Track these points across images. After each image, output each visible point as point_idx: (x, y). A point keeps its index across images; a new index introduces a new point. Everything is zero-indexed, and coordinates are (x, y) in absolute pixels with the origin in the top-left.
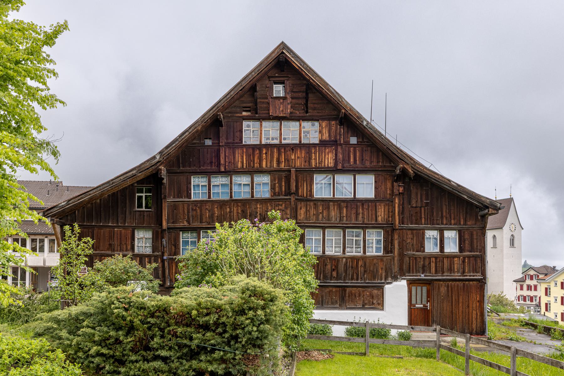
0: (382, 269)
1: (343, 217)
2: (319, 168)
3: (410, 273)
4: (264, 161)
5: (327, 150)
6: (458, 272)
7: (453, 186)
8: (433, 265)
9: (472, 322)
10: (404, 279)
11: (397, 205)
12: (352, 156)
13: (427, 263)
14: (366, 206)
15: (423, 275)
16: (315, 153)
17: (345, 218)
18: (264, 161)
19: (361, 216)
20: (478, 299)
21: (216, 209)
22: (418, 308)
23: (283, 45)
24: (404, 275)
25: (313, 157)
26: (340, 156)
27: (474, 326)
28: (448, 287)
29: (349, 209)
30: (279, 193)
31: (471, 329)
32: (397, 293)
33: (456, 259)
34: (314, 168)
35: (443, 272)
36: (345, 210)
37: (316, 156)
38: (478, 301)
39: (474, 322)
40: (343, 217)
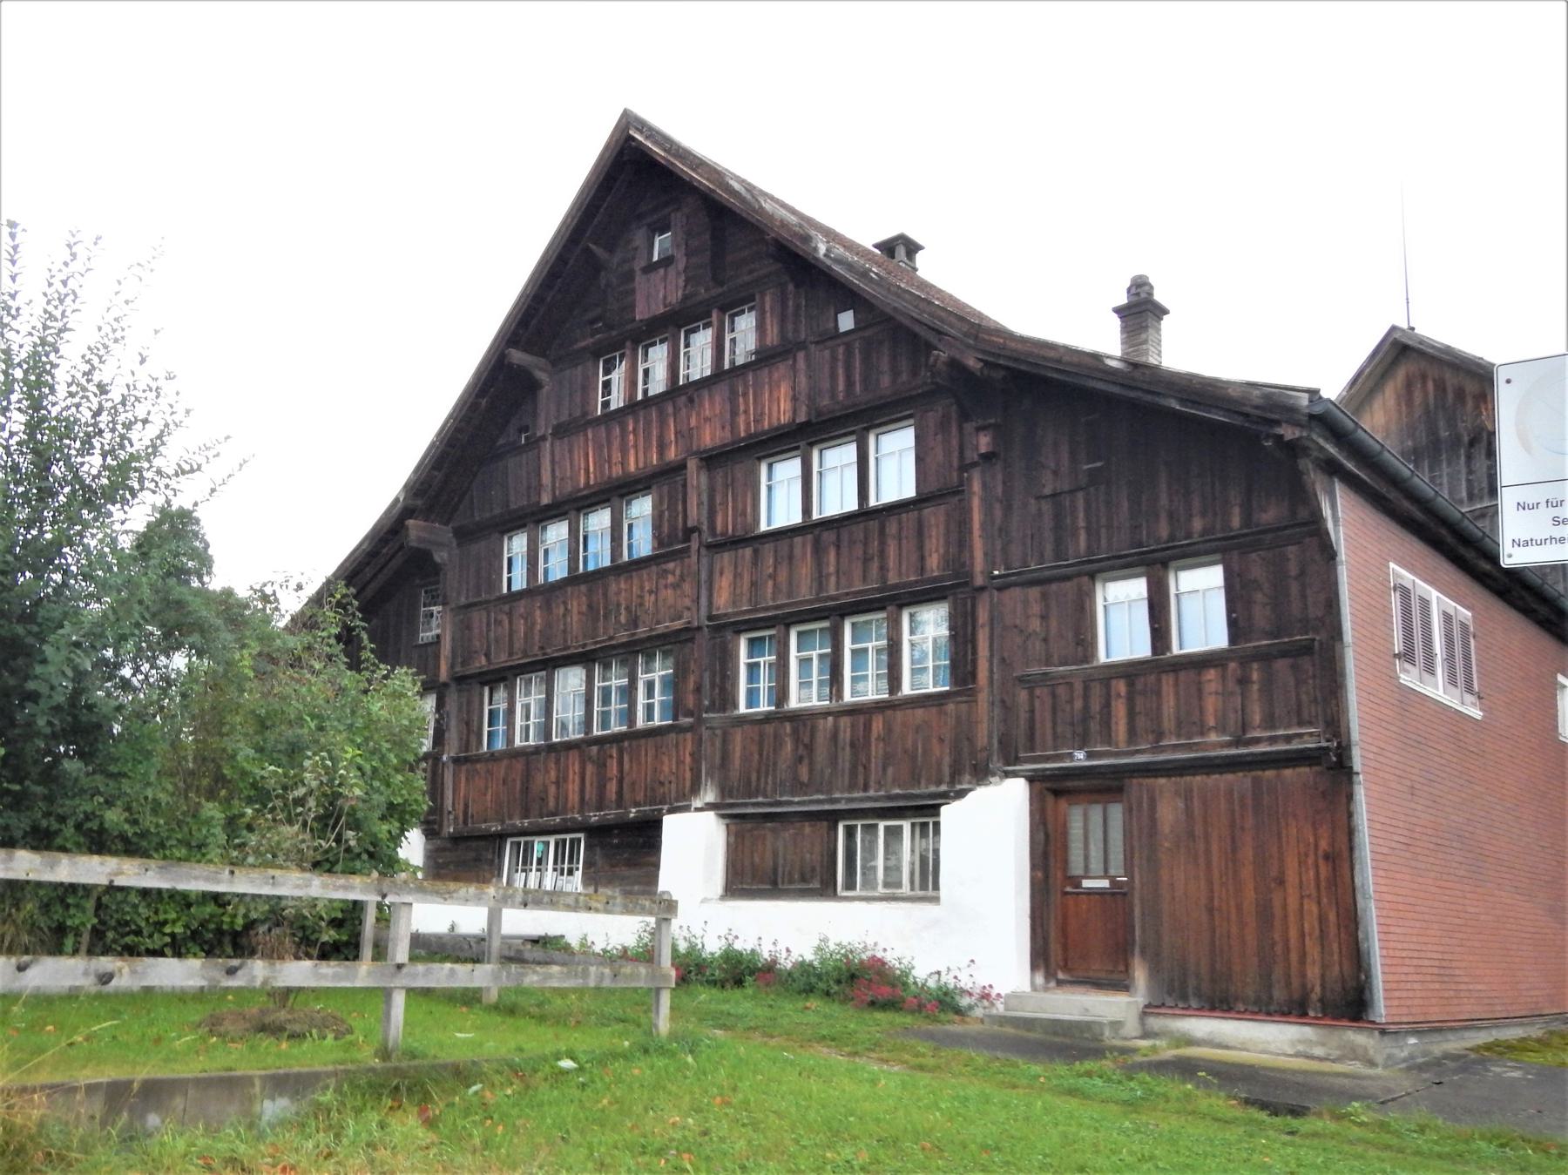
0: (941, 740)
1: (829, 575)
2: (756, 435)
3: (1032, 749)
4: (632, 452)
5: (776, 375)
6: (1221, 728)
7: (1114, 372)
8: (1120, 710)
9: (1303, 956)
10: (1015, 774)
11: (976, 502)
12: (841, 371)
13: (1095, 707)
14: (892, 527)
15: (1080, 755)
16: (745, 394)
17: (833, 579)
18: (632, 452)
19: (875, 565)
20: (1323, 844)
21: (538, 613)
22: (1091, 892)
23: (628, 122)
24: (1018, 761)
25: (742, 408)
26: (803, 380)
27: (1313, 973)
28: (1188, 798)
29: (845, 550)
30: (669, 536)
31: (1296, 982)
32: (988, 827)
33: (1211, 674)
34: (743, 439)
35: (1160, 735)
36: (832, 556)
37: (747, 404)
38: (1327, 857)
39: (1313, 951)
40: (829, 575)
